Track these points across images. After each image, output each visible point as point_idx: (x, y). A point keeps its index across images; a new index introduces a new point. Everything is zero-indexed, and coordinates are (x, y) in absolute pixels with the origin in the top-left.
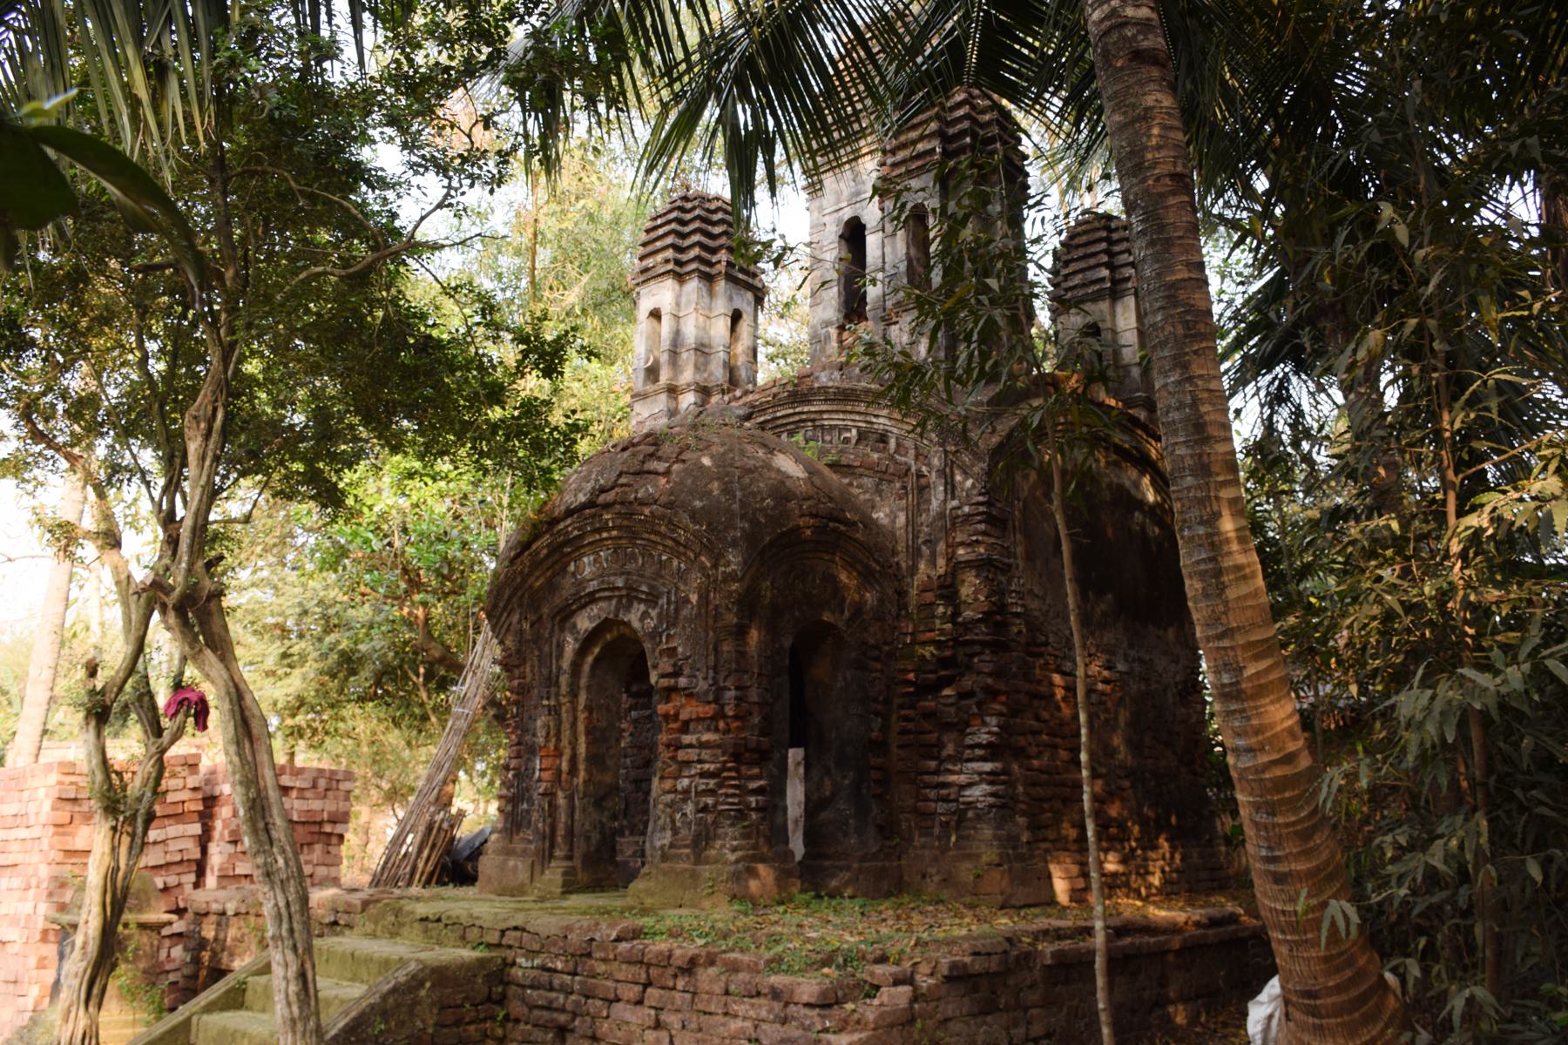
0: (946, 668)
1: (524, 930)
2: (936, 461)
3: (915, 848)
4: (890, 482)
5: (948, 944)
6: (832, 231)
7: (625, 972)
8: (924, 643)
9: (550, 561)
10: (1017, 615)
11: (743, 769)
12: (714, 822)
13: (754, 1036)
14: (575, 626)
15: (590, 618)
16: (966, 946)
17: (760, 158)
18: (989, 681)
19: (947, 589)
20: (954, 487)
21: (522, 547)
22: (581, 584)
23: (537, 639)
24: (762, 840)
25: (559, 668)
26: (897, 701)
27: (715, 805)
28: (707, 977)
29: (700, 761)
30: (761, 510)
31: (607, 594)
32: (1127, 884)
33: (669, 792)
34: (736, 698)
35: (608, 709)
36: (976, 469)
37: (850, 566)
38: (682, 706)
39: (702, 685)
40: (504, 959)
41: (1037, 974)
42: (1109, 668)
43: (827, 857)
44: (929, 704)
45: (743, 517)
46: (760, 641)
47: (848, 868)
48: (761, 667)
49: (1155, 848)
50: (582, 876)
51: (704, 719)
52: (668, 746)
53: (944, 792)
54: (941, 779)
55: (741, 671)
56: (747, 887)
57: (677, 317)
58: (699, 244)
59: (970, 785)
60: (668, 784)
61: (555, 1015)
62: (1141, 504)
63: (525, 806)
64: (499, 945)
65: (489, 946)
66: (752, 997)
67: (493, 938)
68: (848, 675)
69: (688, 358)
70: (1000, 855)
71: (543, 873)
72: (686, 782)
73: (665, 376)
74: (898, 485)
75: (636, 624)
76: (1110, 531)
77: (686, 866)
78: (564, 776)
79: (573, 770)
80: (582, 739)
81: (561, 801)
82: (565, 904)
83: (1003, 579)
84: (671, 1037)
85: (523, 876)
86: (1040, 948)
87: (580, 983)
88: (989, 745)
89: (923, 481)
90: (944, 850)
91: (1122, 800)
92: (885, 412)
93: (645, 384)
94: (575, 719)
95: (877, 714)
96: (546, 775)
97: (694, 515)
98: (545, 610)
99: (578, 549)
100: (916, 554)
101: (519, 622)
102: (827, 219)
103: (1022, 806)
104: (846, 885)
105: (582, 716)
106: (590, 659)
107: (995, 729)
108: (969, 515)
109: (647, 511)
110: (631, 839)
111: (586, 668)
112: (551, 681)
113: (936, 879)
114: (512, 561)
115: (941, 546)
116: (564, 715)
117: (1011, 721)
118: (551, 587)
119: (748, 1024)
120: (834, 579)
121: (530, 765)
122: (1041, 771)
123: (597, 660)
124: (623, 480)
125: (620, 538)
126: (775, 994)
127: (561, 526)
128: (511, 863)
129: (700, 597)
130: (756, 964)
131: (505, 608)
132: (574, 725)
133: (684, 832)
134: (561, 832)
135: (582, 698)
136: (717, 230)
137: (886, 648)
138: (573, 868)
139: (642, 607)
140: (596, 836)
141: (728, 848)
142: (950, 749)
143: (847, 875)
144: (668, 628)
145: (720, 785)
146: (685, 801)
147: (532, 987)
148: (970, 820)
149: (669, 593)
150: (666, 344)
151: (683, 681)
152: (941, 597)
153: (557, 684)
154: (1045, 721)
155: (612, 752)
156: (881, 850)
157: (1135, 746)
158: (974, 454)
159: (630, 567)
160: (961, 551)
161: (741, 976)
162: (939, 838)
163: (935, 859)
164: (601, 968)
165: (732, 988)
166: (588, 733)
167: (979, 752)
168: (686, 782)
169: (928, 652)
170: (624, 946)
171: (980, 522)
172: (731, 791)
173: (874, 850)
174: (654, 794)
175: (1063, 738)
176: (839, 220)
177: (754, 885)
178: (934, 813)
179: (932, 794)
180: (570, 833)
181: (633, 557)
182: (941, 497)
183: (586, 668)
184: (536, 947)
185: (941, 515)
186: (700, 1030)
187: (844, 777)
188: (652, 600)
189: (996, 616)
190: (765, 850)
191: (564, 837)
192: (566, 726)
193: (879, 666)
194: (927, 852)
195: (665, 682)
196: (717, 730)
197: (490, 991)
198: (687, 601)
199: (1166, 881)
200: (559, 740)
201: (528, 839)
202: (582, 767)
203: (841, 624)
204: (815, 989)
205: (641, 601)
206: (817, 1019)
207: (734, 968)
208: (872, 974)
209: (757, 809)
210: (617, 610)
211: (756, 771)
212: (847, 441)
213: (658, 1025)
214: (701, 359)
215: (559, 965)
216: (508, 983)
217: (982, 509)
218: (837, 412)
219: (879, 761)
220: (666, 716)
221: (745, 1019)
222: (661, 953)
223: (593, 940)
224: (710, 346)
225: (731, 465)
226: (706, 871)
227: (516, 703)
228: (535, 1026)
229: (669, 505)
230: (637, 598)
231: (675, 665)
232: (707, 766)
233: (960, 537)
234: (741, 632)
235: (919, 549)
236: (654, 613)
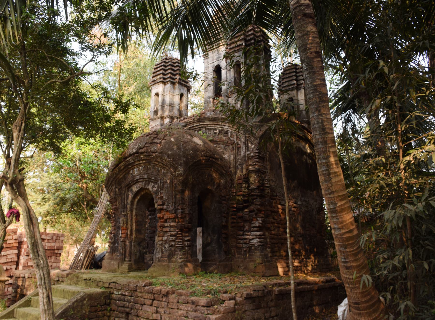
0: (245, 203)
1: (116, 283)
2: (243, 140)
3: (236, 258)
4: (229, 146)
5: (246, 288)
6: (211, 69)
7: (147, 296)
8: (239, 195)
9: (124, 170)
10: (268, 187)
11: (183, 234)
12: (174, 250)
13: (186, 315)
14: (132, 190)
15: (136, 187)
16: (251, 288)
17: (189, 47)
18: (259, 207)
19: (246, 179)
20: (248, 148)
21: (116, 165)
22: (134, 177)
23: (120, 194)
24: (189, 255)
25: (127, 203)
26: (231, 213)
27: (175, 245)
28: (172, 297)
29: (170, 231)
30: (189, 154)
31: (142, 180)
32: (301, 270)
33: (161, 241)
34: (181, 212)
35: (142, 215)
36: (255, 142)
37: (216, 172)
38: (165, 215)
39: (171, 208)
40: (110, 292)
41: (273, 297)
42: (296, 203)
43: (209, 261)
44: (240, 214)
45: (184, 157)
46: (189, 195)
47: (215, 264)
48: (189, 203)
49: (310, 258)
50: (134, 267)
51: (171, 218)
52: (160, 227)
53: (245, 241)
54: (244, 237)
55: (183, 204)
56: (184, 270)
57: (163, 95)
58: (170, 73)
59: (253, 239)
60: (160, 238)
61: (126, 309)
62: (306, 153)
63: (117, 245)
64: (108, 288)
65: (105, 288)
66: (186, 304)
67: (107, 285)
68: (216, 205)
69: (167, 108)
70: (262, 260)
71: (122, 265)
72: (166, 238)
73: (160, 113)
74: (231, 147)
75: (151, 189)
76: (296, 161)
77: (166, 263)
78: (129, 236)
79: (131, 234)
80: (134, 224)
81: (128, 243)
82: (129, 275)
83: (263, 176)
84: (161, 316)
85: (116, 266)
86: (274, 289)
87: (133, 299)
88: (259, 227)
89: (239, 146)
90: (245, 259)
91: (300, 244)
92: (227, 125)
93: (154, 116)
94: (132, 218)
95: (224, 217)
96: (123, 235)
97: (169, 156)
98: (123, 185)
99: (133, 166)
100: (237, 168)
101: (115, 188)
102: (209, 65)
103: (269, 246)
104: (215, 270)
105: (134, 217)
106: (136, 200)
107: (261, 222)
108: (253, 156)
109: (154, 155)
110: (149, 255)
111: (135, 203)
112: (125, 207)
113: (242, 268)
114: (113, 170)
115: (244, 166)
116: (129, 217)
117: (266, 219)
118: (125, 178)
119: (185, 312)
120: (211, 176)
121: (118, 232)
122: (274, 235)
123: (139, 200)
124: (147, 145)
125: (146, 163)
126: (193, 303)
127: (128, 159)
128: (112, 262)
129: (170, 181)
130: (187, 294)
131: (111, 184)
132: (132, 220)
133: (165, 253)
135: (134, 212)
136: (176, 69)
137: (227, 197)
138: (131, 264)
139: (153, 184)
140: (138, 254)
141: (179, 258)
142: (247, 228)
143: (215, 266)
144: (160, 191)
145: (176, 239)
146: (165, 243)
147: (118, 300)
148: (253, 250)
149: (161, 180)
150: (160, 103)
151: (165, 207)
152: (244, 181)
153: (127, 208)
154: (276, 220)
155: (143, 228)
156: (225, 259)
157: (303, 227)
158: (255, 137)
159: (149, 172)
160: (250, 167)
161: (183, 297)
162: (243, 255)
163: (242, 262)
164: (140, 295)
165: (180, 301)
166: (136, 223)
167: (256, 229)
168: (166, 238)
169: (240, 198)
170: (146, 288)
171: (256, 158)
172: (180, 240)
173: (223, 259)
174: (156, 241)
175: (281, 225)
176: (213, 66)
177: (186, 269)
178: (241, 248)
179: (241, 242)
180: (130, 253)
181: (150, 169)
182: (244, 151)
183: (135, 203)
184: (120, 288)
185: (244, 156)
186: (170, 314)
187: (214, 236)
188: (155, 182)
189: (261, 187)
190: (190, 259)
191: (128, 254)
192: (129, 220)
193: (225, 202)
194: (240, 260)
195: (159, 207)
196: (175, 222)
197: (106, 302)
198: (166, 182)
199: (313, 269)
200: (127, 225)
201: (117, 255)
202: (134, 233)
203: (213, 190)
204: (205, 301)
205: (152, 182)
206: (206, 311)
207: (180, 295)
208: (223, 297)
209: (188, 246)
211: (187, 234)
212: (215, 133)
213: (157, 312)
214: (171, 108)
215: (127, 294)
216: (111, 299)
217: (257, 154)
218: (212, 124)
219: (225, 231)
220: (160, 218)
221: (183, 310)
222: (158, 290)
223: (137, 286)
224: (174, 104)
225: (180, 141)
226: (172, 265)
227: (114, 213)
228: (119, 312)
229: (161, 153)
230: (151, 181)
231: (162, 202)
232: (172, 233)
233: (250, 163)
234: (183, 192)
235: (237, 167)
236: (156, 186)
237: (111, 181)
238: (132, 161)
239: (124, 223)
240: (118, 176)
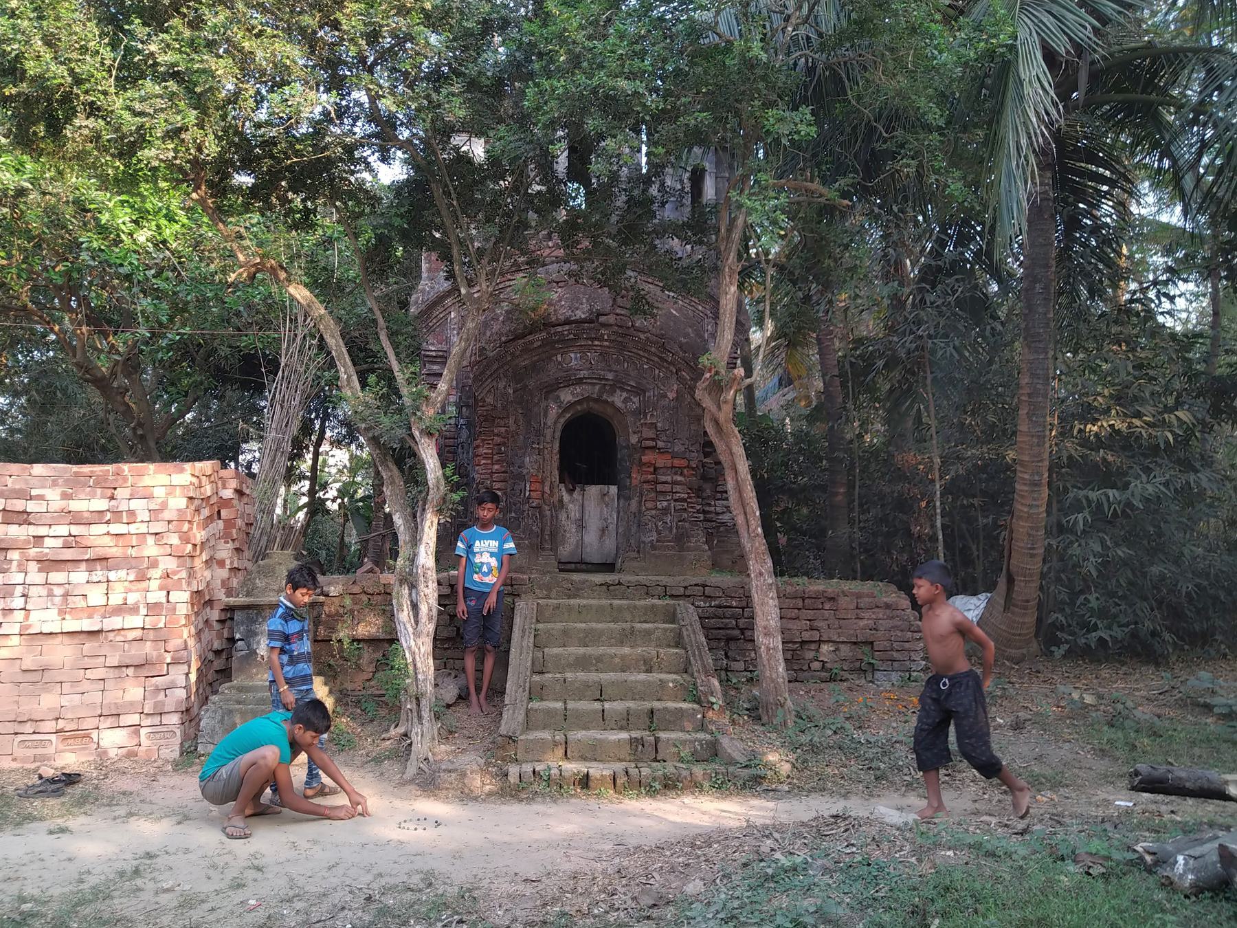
14: (558, 397)
109: (642, 336)
139: (625, 394)
188: (639, 391)
196: (681, 474)
238: (571, 336)
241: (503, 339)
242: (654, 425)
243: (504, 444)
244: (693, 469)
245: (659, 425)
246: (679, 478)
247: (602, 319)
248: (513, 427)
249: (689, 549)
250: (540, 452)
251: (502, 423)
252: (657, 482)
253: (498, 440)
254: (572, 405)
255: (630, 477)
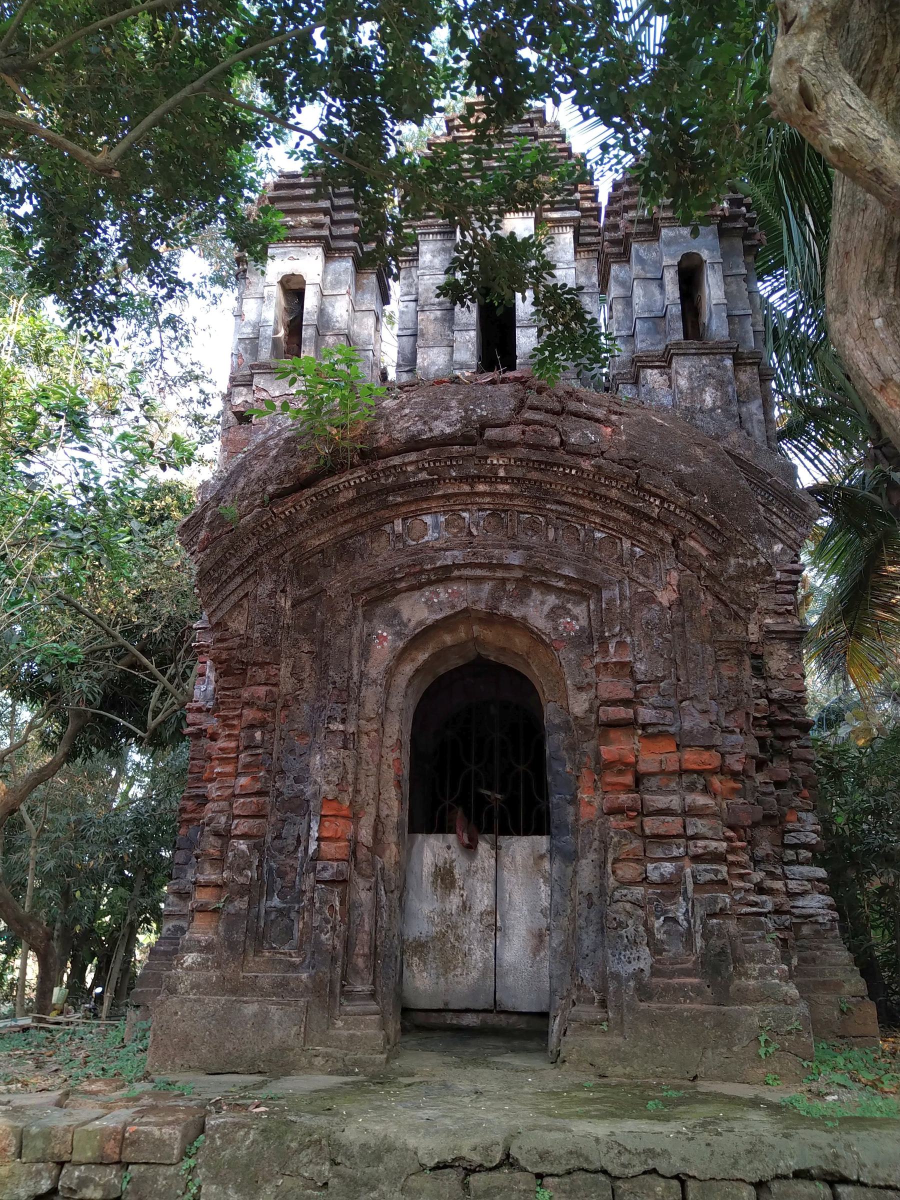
14: (396, 613)
109: (586, 464)
125: (511, 496)
128: (250, 1009)
131: (241, 569)
134: (362, 948)
139: (552, 600)
160: (768, 621)
188: (585, 588)
196: (707, 790)
210: (495, 599)
237: (249, 551)
238: (424, 476)
239: (343, 778)
240: (301, 536)
241: (270, 489)
242: (625, 669)
243: (262, 725)
244: (735, 775)
245: (641, 667)
246: (701, 800)
247: (491, 433)
248: (287, 684)
249: (744, 997)
250: (348, 741)
251: (261, 675)
252: (643, 812)
253: (249, 714)
254: (427, 632)
255: (574, 801)
